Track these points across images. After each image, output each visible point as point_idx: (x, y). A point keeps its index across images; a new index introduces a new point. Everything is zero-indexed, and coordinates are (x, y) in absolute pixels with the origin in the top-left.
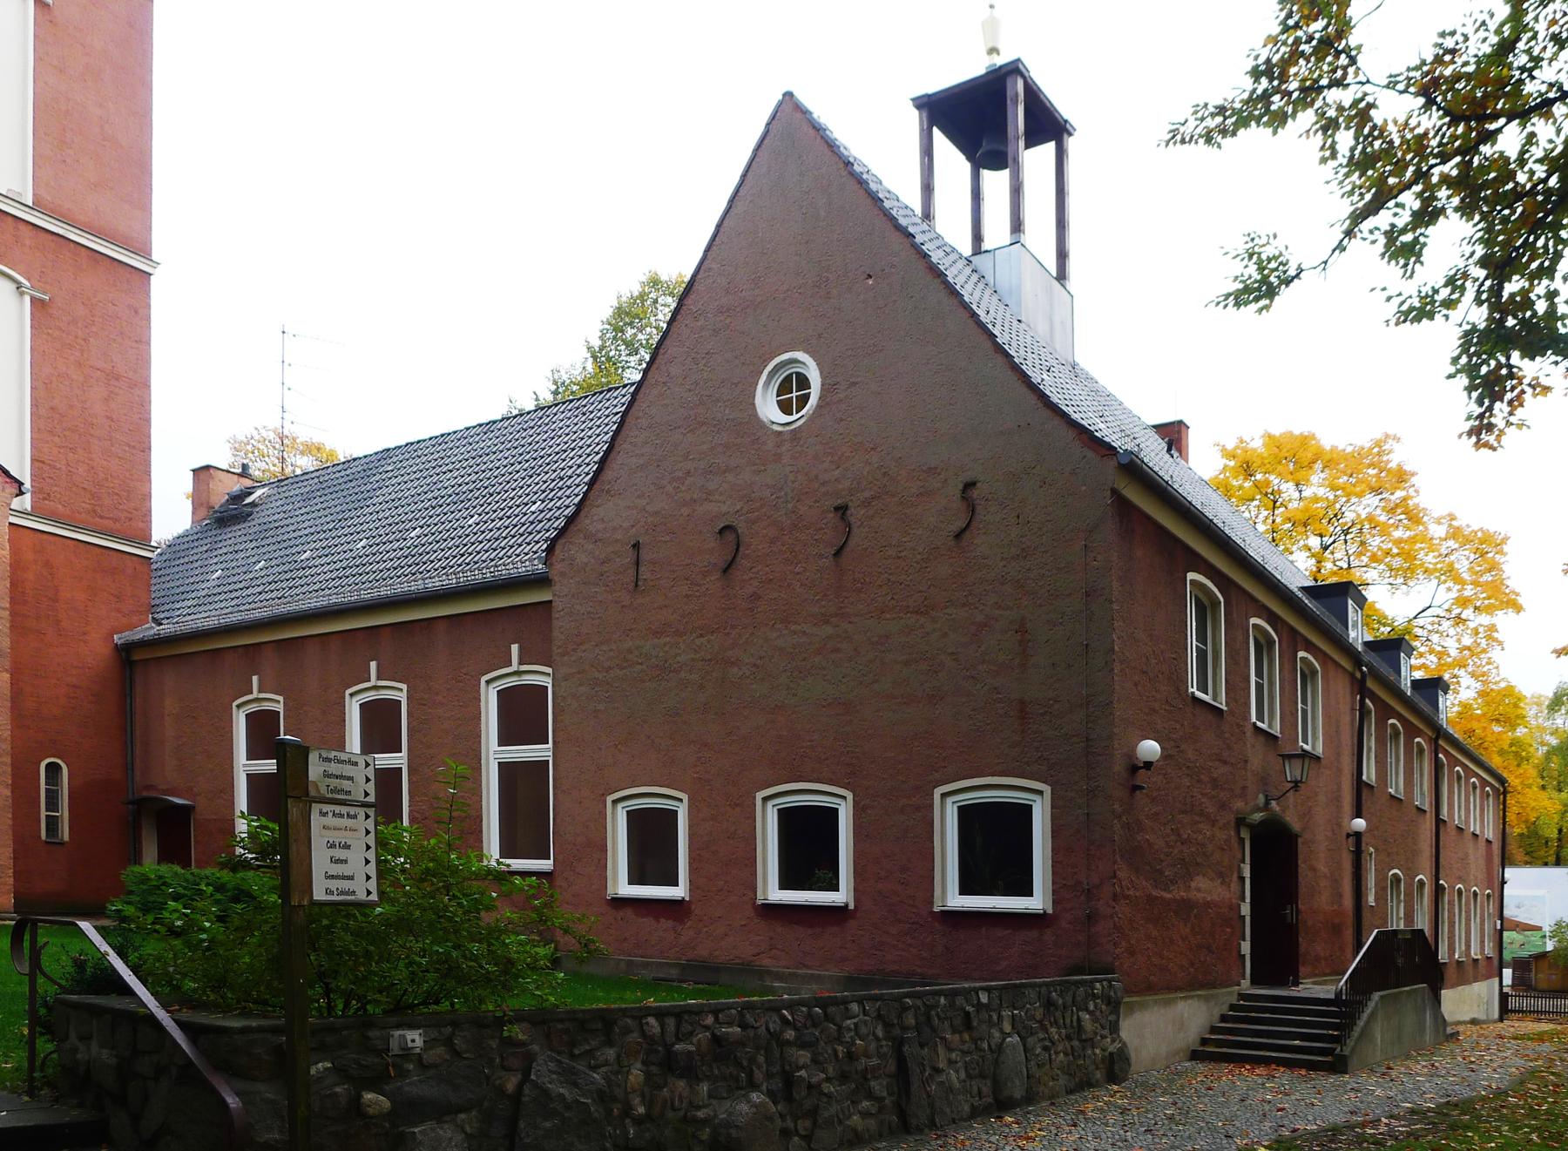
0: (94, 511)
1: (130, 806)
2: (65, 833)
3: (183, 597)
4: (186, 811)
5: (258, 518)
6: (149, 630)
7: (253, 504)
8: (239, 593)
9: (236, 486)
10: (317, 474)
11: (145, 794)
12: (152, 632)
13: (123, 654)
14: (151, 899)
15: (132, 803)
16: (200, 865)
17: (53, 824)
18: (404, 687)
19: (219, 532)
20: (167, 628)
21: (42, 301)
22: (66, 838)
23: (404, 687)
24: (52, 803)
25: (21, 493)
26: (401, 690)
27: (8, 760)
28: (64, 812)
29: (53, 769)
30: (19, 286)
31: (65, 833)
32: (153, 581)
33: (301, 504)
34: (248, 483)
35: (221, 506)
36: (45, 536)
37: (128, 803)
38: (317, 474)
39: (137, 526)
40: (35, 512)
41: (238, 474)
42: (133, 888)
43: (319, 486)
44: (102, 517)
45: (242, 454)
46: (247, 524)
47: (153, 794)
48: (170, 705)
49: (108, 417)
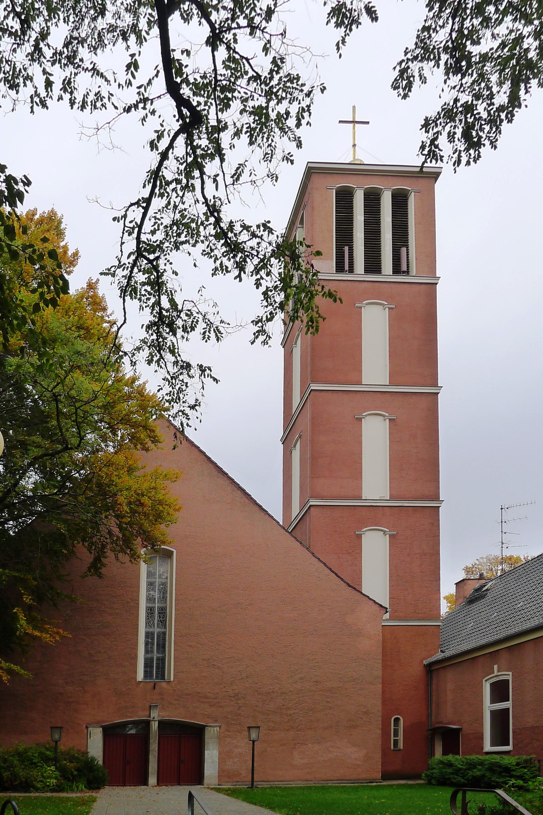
0: (415, 612)
1: (430, 732)
2: (401, 746)
3: (454, 638)
4: (458, 731)
5: (490, 595)
6: (439, 656)
7: (487, 590)
8: (484, 630)
9: (477, 585)
10: (523, 566)
11: (437, 726)
12: (441, 656)
13: (428, 668)
14: (444, 771)
15: (431, 730)
16: (464, 754)
17: (396, 742)
18: (510, 673)
19: (470, 606)
20: (448, 654)
21: (393, 535)
22: (402, 748)
23: (510, 673)
24: (396, 734)
25: (387, 612)
26: (509, 675)
27: (380, 719)
28: (401, 737)
29: (397, 720)
30: (384, 532)
31: (401, 746)
32: (441, 634)
33: (515, 582)
34: (483, 581)
35: (470, 595)
36: (395, 627)
37: (429, 730)
38: (523, 566)
39: (435, 613)
40: (391, 619)
41: (479, 579)
42: (435, 766)
43: (524, 572)
44: (419, 614)
45: (471, 573)
46: (485, 599)
47: (441, 725)
48: (450, 686)
49: (421, 572)
